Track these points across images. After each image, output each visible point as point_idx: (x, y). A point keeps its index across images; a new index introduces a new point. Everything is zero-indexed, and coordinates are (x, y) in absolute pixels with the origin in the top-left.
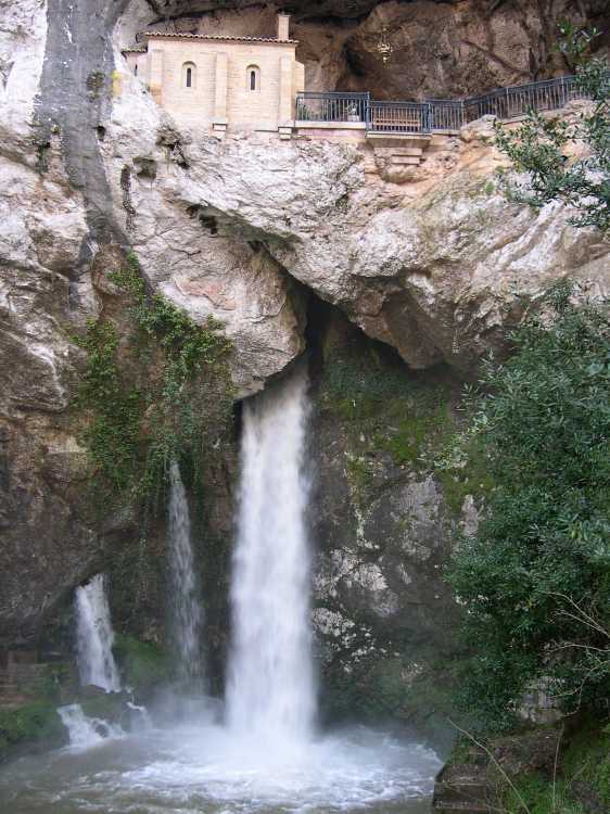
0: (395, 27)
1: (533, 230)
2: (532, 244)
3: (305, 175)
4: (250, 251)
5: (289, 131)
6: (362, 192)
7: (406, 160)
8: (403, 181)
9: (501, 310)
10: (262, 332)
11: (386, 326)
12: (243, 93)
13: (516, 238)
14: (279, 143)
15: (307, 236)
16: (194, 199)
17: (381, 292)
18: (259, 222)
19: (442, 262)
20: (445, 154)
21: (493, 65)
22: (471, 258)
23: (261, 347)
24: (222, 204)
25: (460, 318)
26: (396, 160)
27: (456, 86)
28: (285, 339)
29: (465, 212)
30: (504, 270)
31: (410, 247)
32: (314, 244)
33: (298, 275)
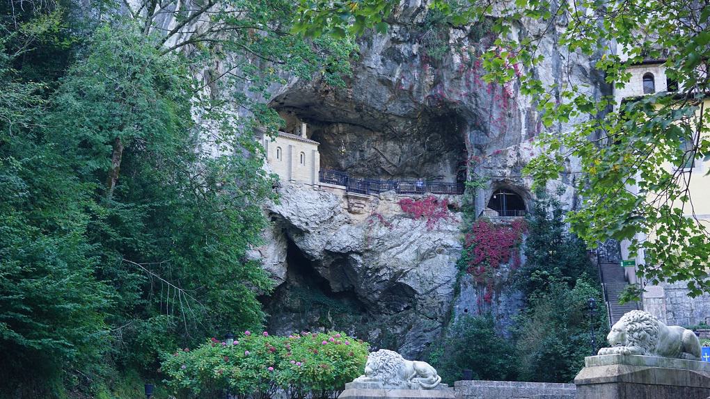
0: (344, 134)
1: (407, 243)
2: (406, 249)
3: (320, 206)
4: (280, 232)
5: (318, 187)
6: (339, 216)
7: (359, 205)
8: (354, 213)
9: (390, 274)
10: (275, 269)
11: (329, 272)
12: (300, 166)
13: (399, 245)
14: (312, 191)
15: (313, 231)
16: (275, 211)
17: (333, 257)
18: (296, 223)
19: (367, 251)
20: (373, 204)
21: (382, 159)
22: (380, 251)
23: (273, 276)
24: (285, 214)
25: (370, 275)
26: (356, 205)
27: (362, 163)
28: (284, 273)
29: (384, 233)
30: (393, 257)
31: (357, 243)
32: (314, 235)
33: (300, 245)
